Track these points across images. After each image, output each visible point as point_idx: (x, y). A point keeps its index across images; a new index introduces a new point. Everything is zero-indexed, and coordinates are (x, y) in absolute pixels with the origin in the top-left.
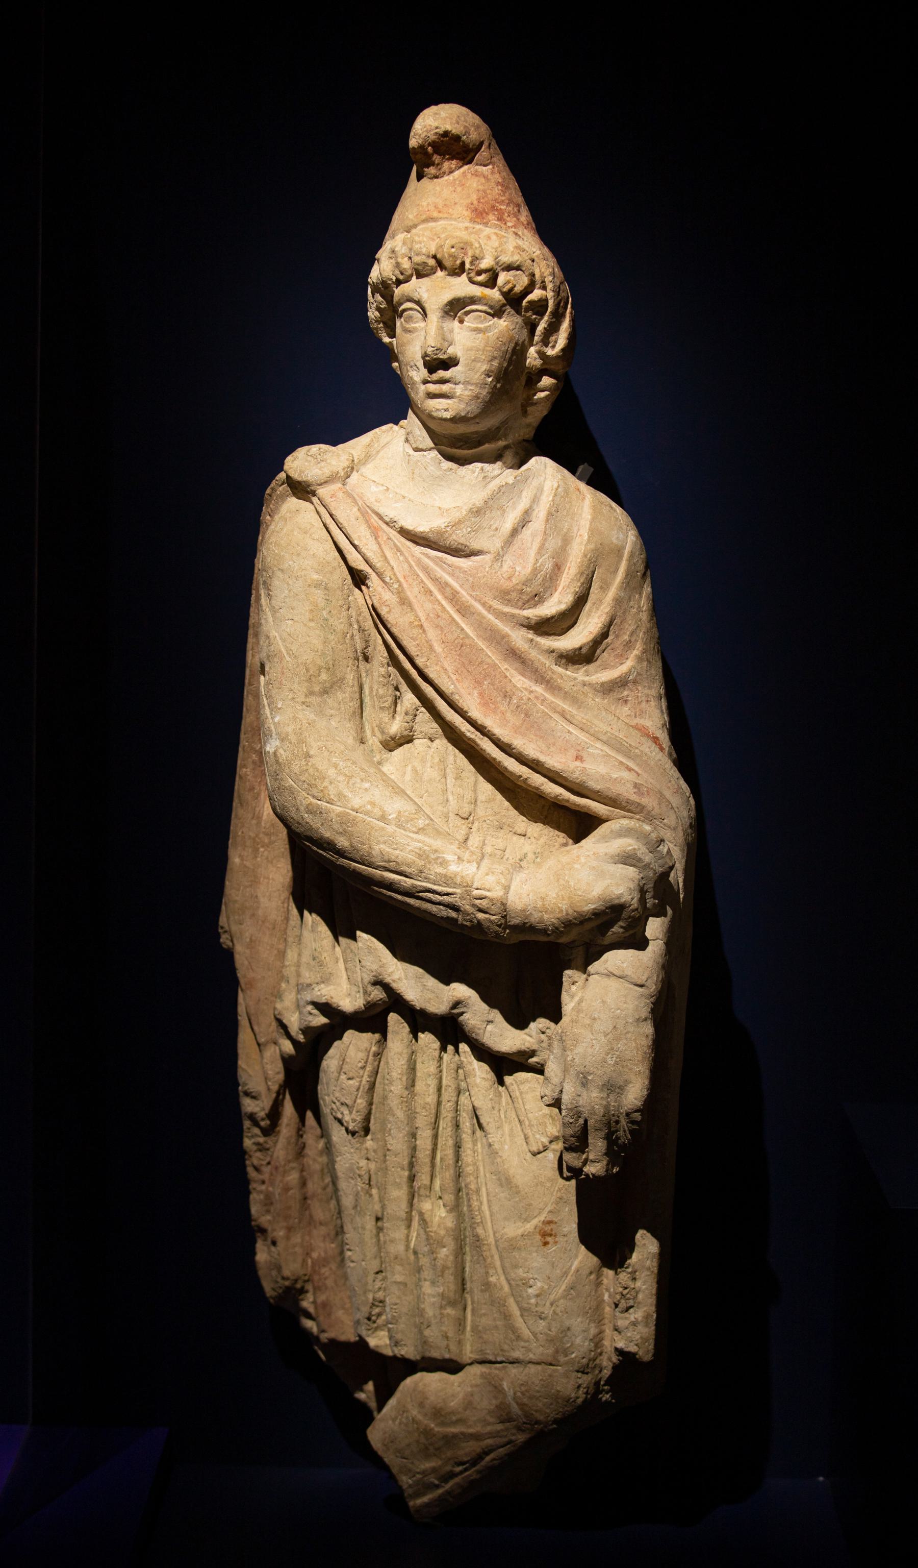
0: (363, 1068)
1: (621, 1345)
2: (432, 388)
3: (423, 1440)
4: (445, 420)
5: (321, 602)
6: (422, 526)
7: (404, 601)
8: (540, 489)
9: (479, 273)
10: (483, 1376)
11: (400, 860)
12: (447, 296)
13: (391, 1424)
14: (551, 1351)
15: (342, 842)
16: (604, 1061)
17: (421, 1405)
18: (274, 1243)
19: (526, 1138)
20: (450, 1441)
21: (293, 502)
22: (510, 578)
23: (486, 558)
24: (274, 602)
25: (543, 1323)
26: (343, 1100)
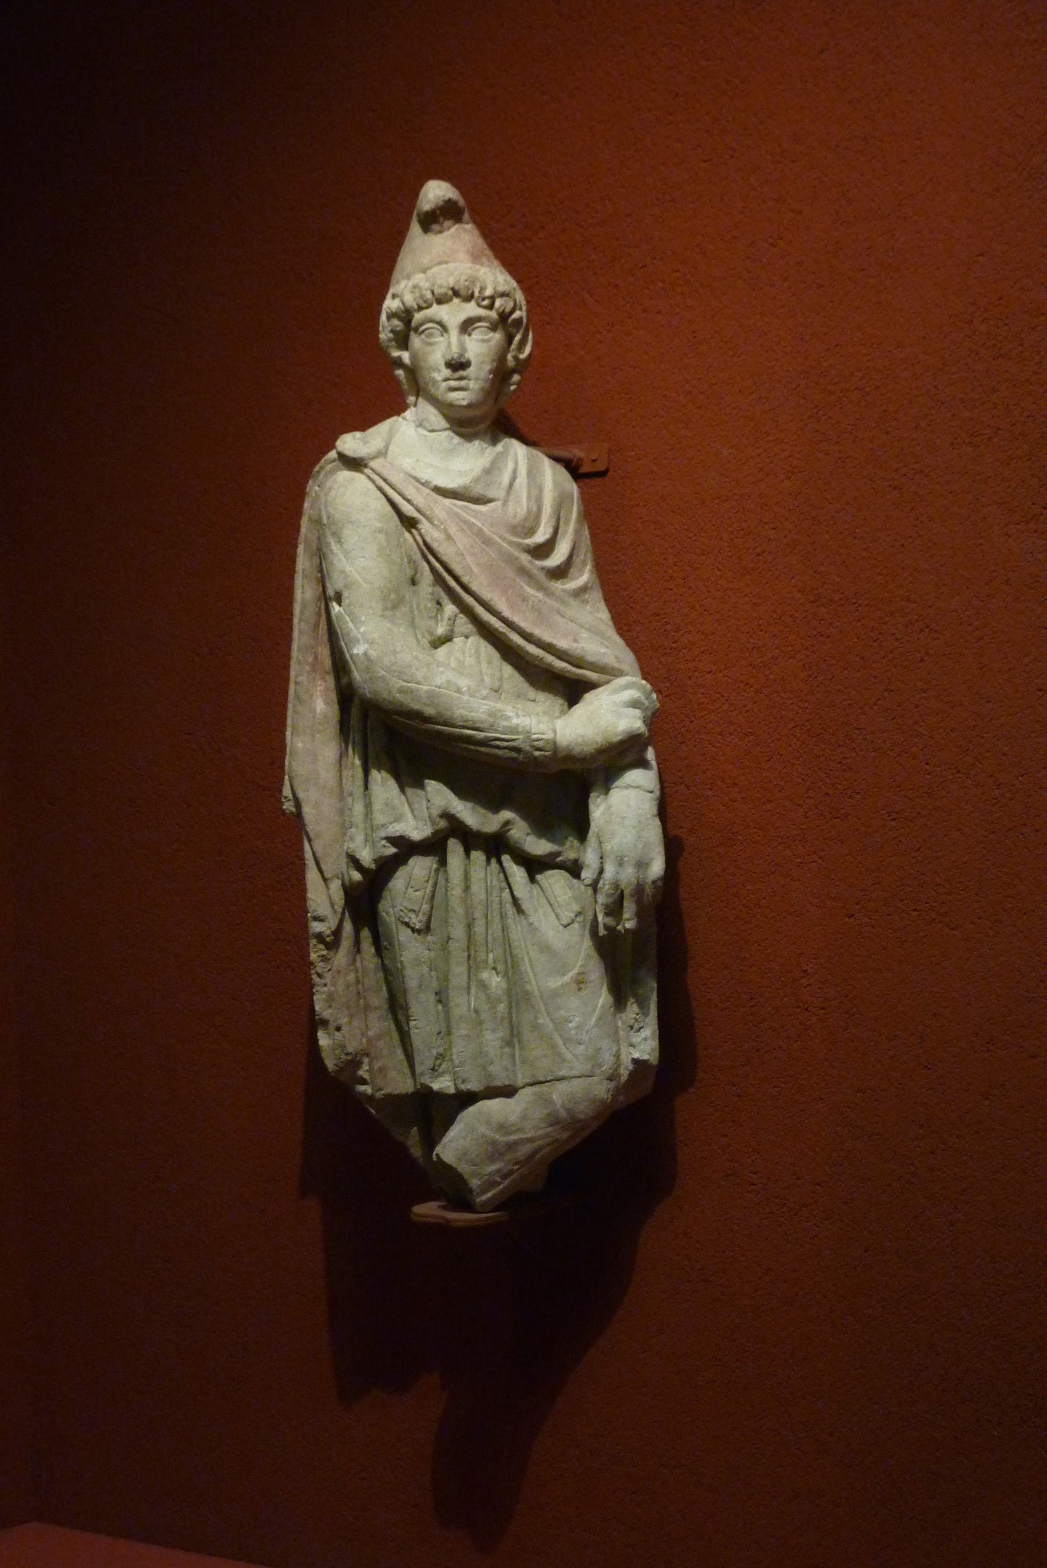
0: (427, 881)
1: (636, 1055)
2: (453, 383)
3: (490, 1149)
4: (464, 407)
5: (385, 544)
7: (449, 537)
8: (516, 454)
9: (484, 299)
10: (534, 1094)
12: (462, 317)
13: (458, 1144)
14: (588, 1066)
15: (429, 711)
16: (635, 845)
17: (488, 1123)
18: (338, 1029)
19: (557, 916)
20: (511, 1146)
21: (345, 475)
23: (499, 503)
24: (345, 546)
25: (582, 1047)
26: (411, 907)
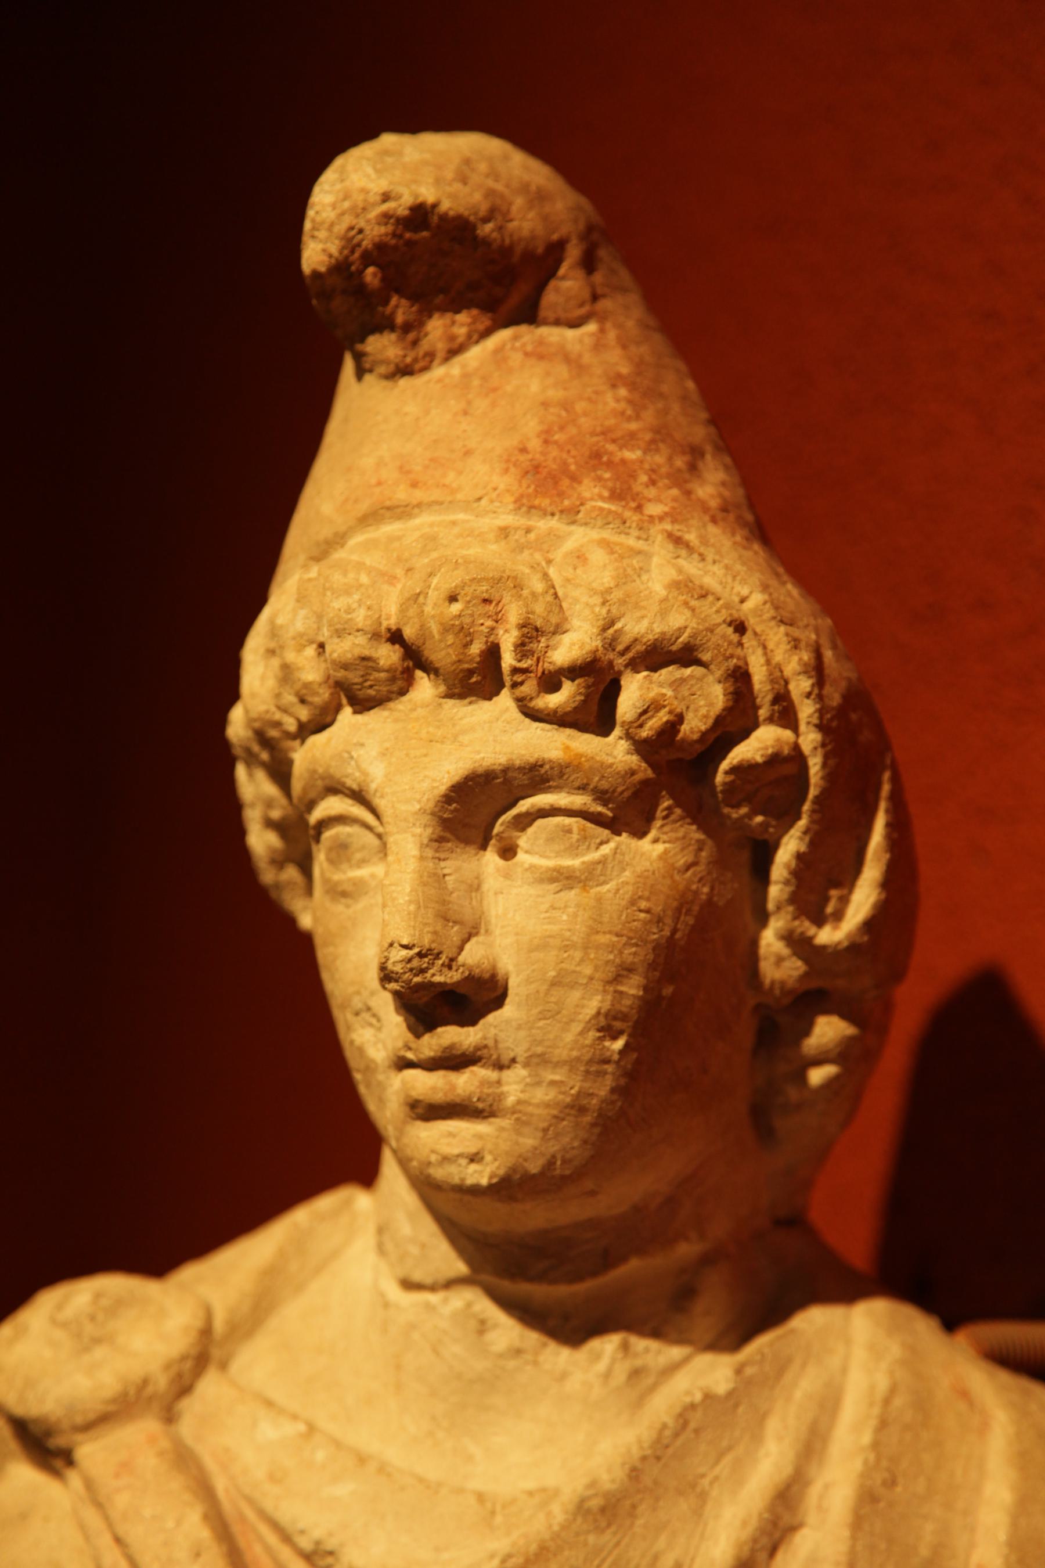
2: (425, 1084)
4: (475, 1191)
8: (829, 1404)
9: (551, 682)
12: (448, 768)
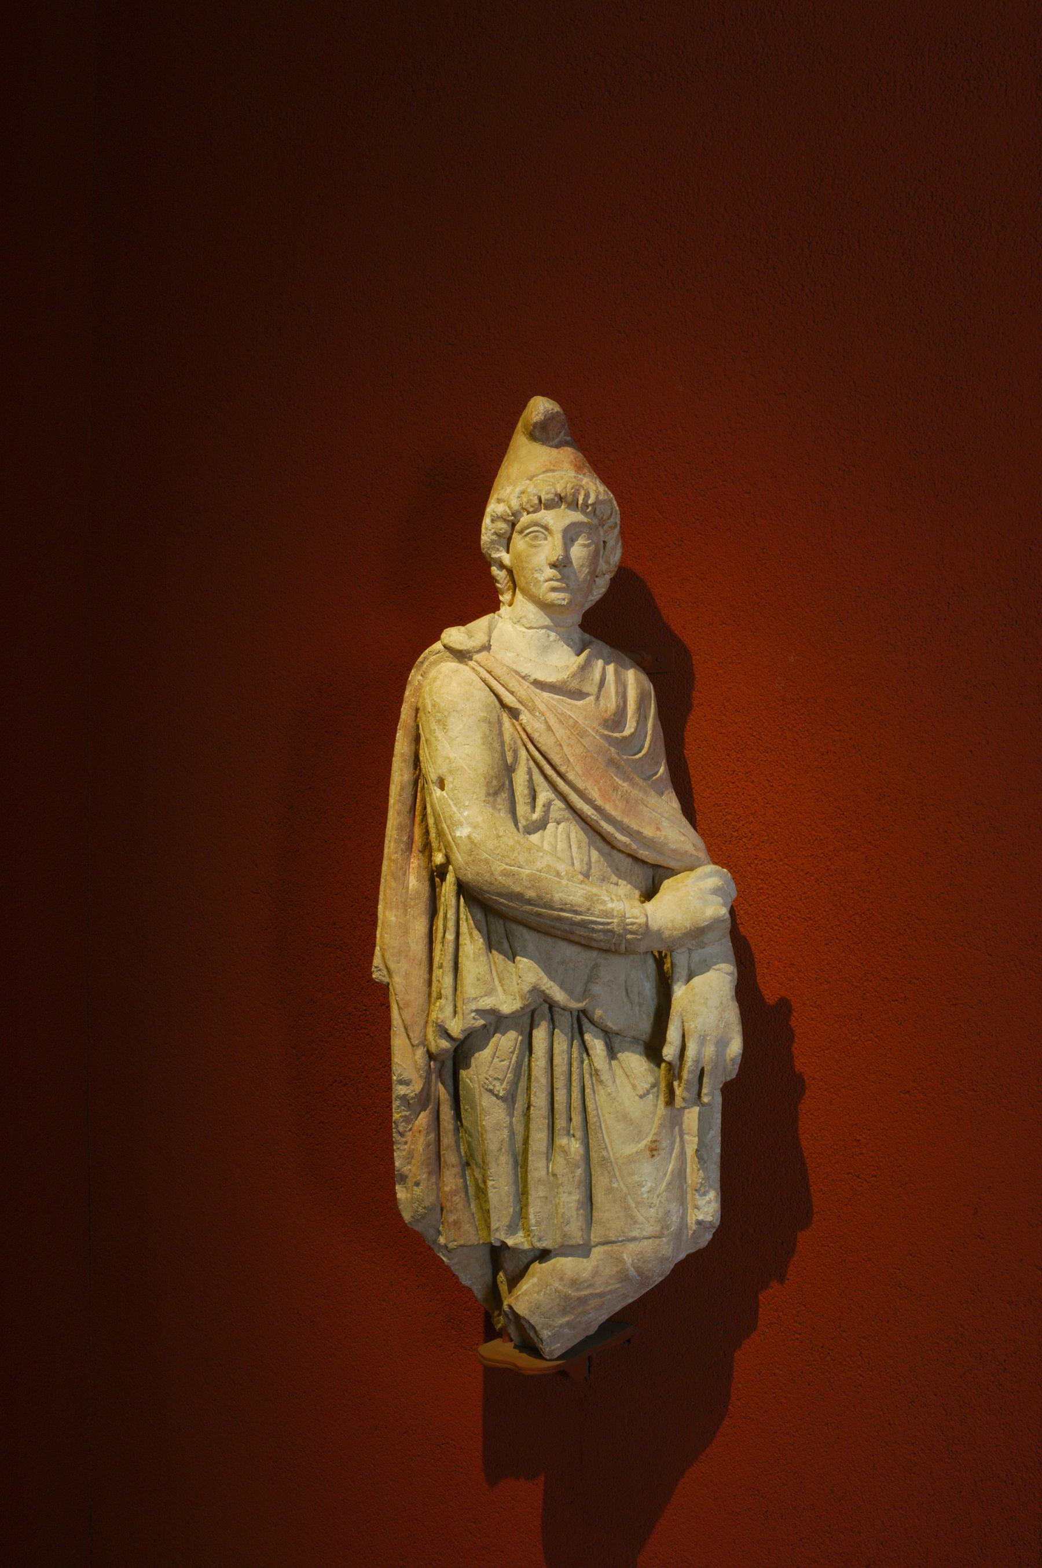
0: (513, 1053)
1: (701, 1217)
3: (563, 1303)
5: (488, 733)
6: (552, 678)
7: (549, 728)
10: (604, 1252)
11: (574, 902)
13: (529, 1296)
14: (658, 1228)
15: (531, 894)
16: (718, 1025)
17: (561, 1279)
18: (417, 1184)
19: (634, 1087)
20: (582, 1301)
21: (450, 666)
22: (606, 711)
23: (592, 698)
24: (450, 734)
25: (652, 1210)
26: (496, 1076)
